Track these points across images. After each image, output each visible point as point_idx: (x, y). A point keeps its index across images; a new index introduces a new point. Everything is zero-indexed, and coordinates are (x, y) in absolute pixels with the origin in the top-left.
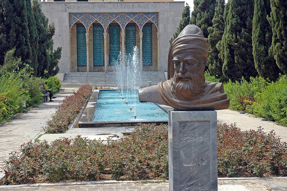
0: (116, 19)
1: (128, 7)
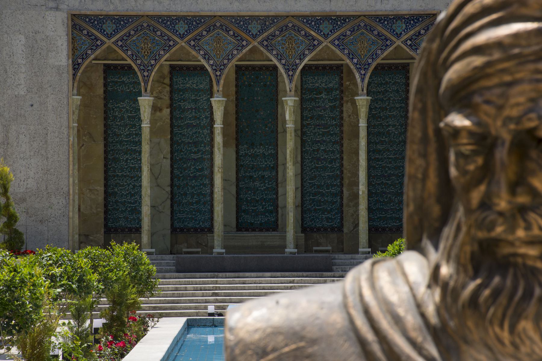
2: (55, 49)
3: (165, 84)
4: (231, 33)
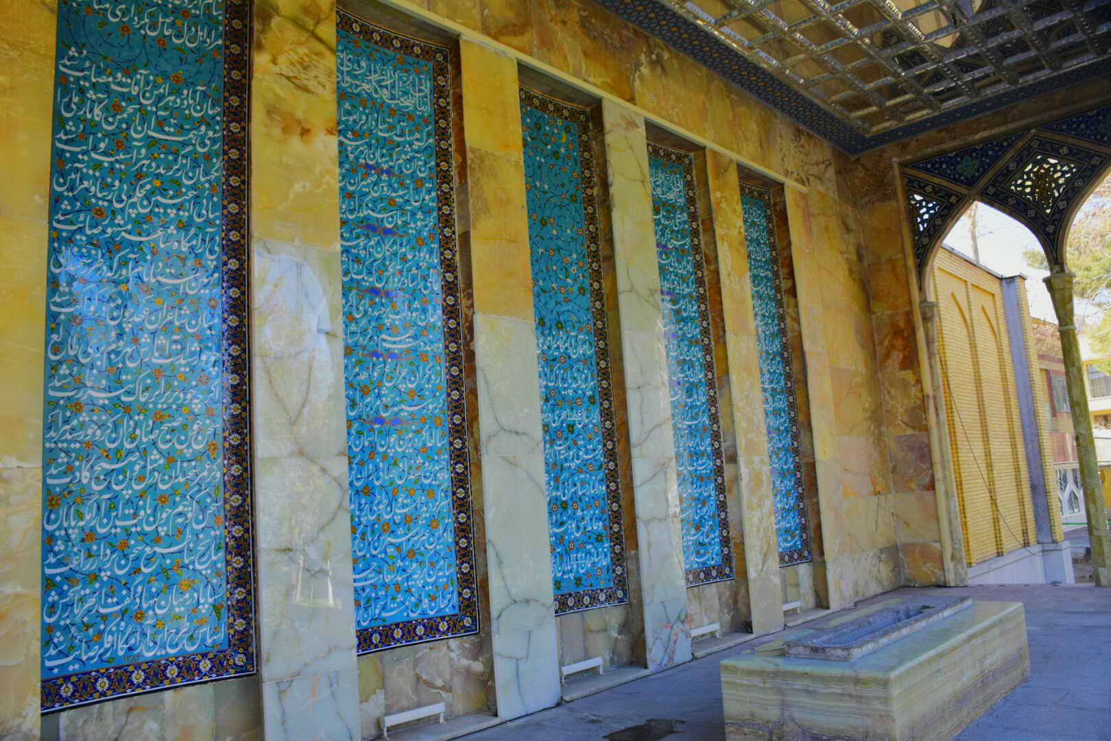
3: (320, 40)
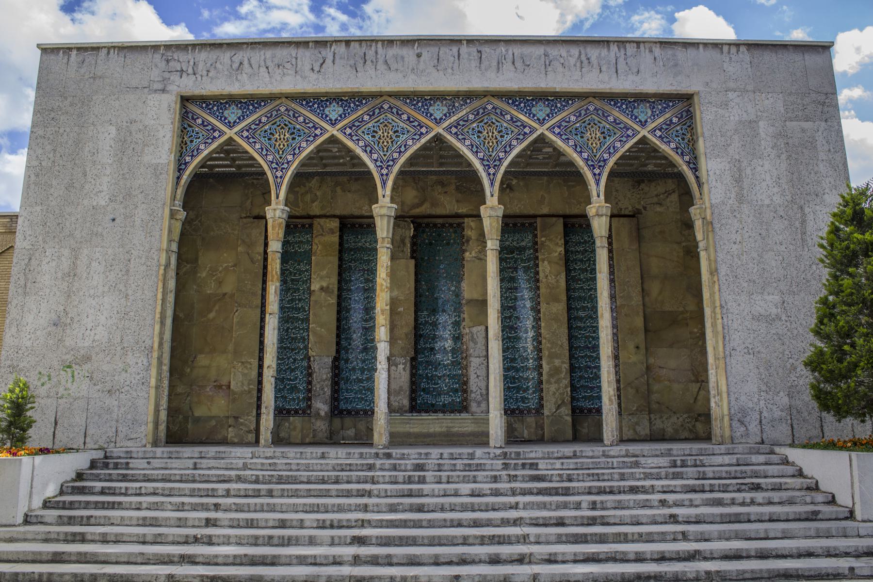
0: (448, 129)
1: (519, 64)
2: (154, 142)
4: (405, 117)
